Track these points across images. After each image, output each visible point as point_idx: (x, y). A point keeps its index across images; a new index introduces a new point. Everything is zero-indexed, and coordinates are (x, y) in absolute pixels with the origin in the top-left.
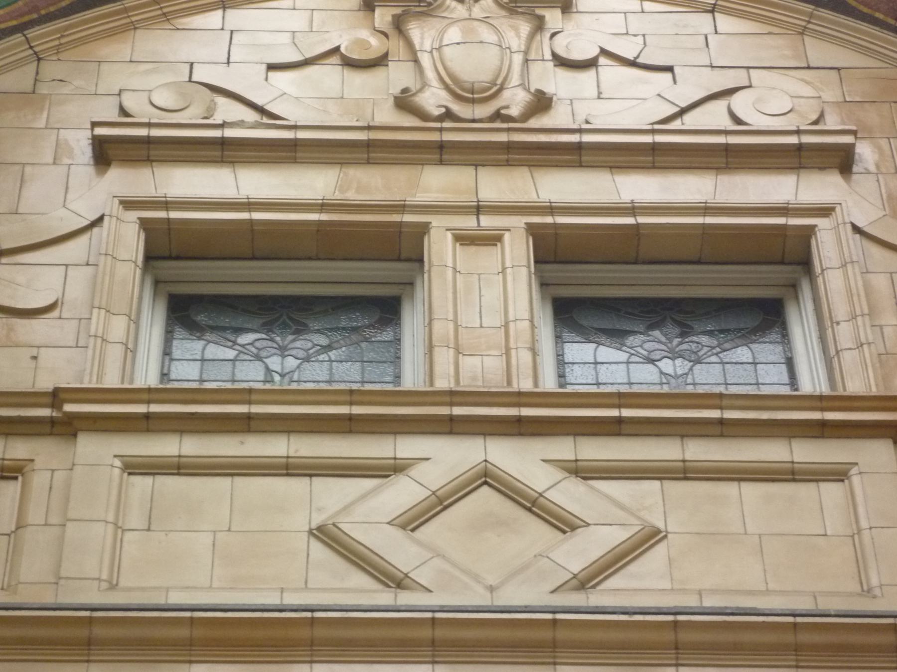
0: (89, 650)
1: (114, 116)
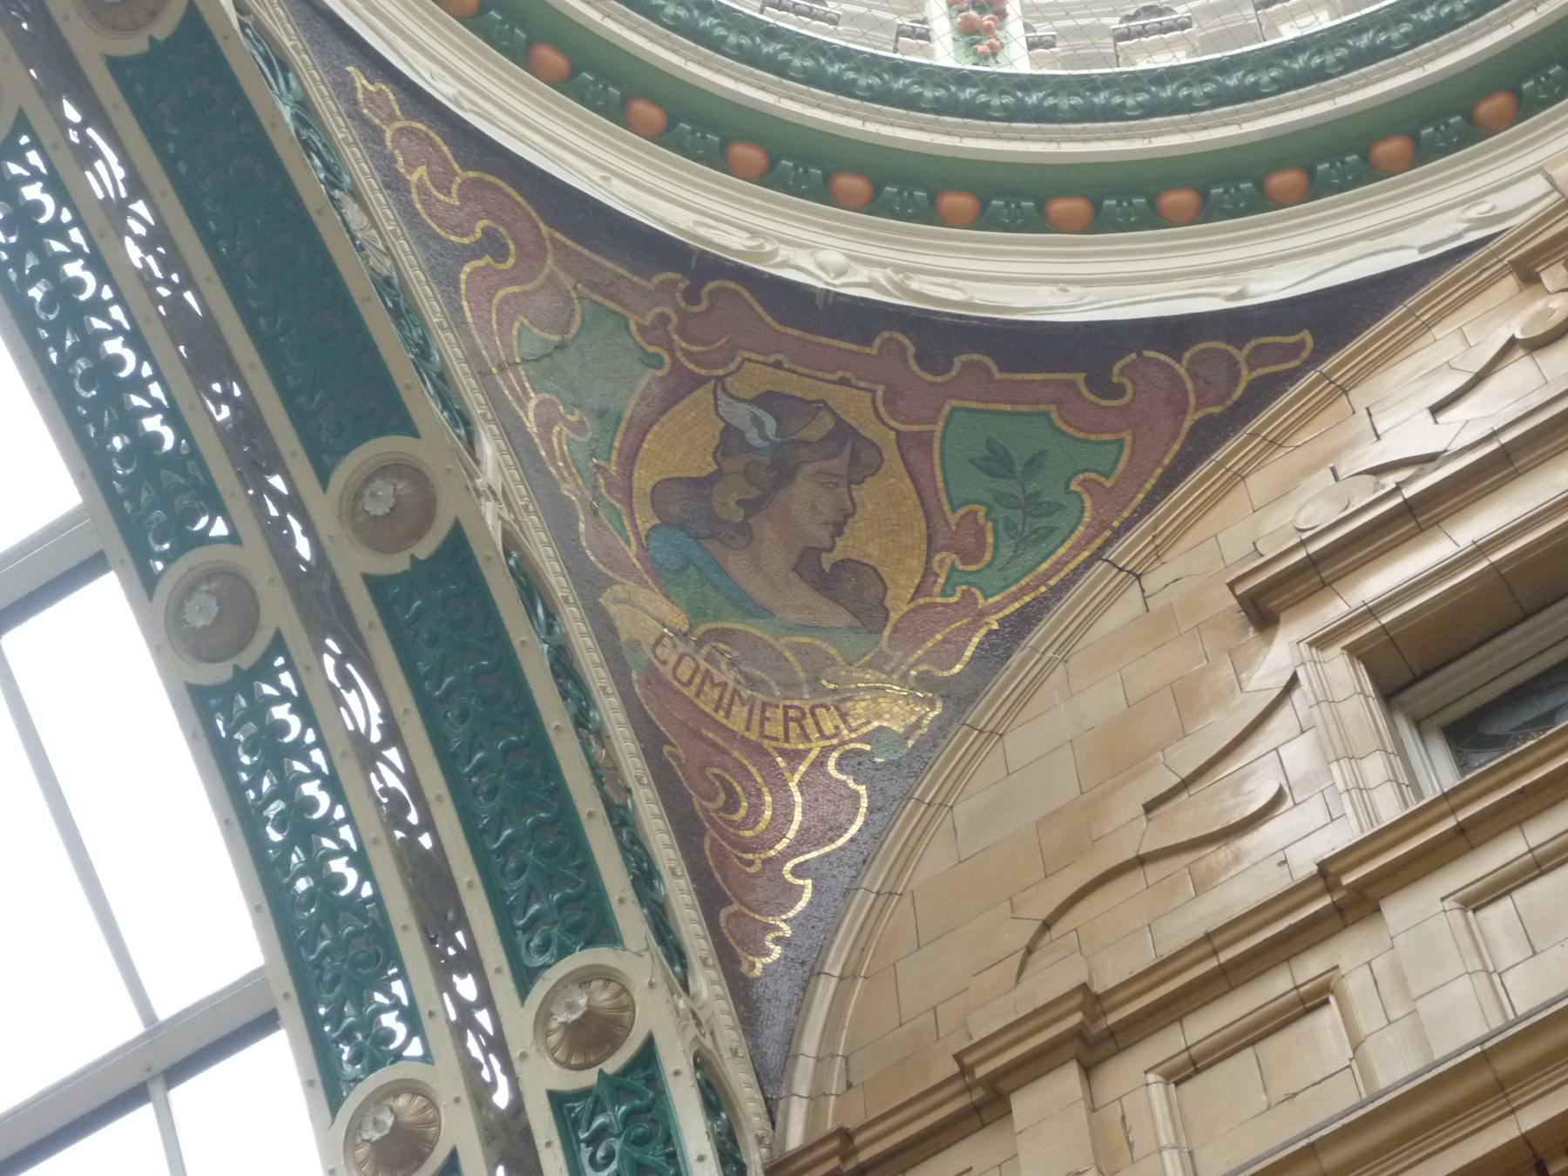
0: (1506, 1095)
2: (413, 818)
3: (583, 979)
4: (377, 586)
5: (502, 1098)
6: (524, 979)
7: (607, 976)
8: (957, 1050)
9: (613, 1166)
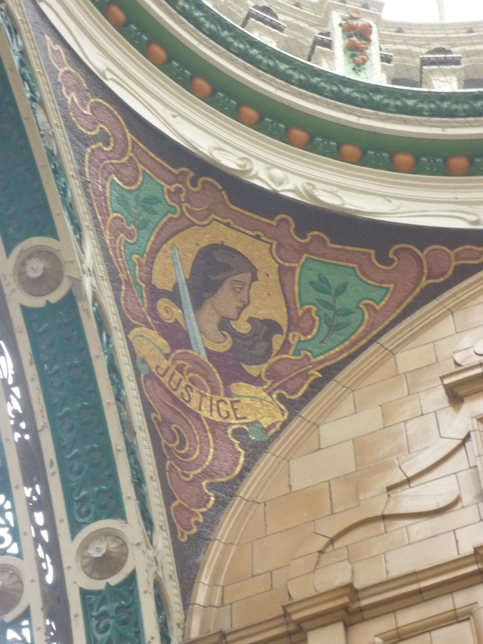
1: (454, 369)
4: (26, 311)
5: (50, 578)
6: (75, 528)
8: (284, 604)
9: (108, 633)
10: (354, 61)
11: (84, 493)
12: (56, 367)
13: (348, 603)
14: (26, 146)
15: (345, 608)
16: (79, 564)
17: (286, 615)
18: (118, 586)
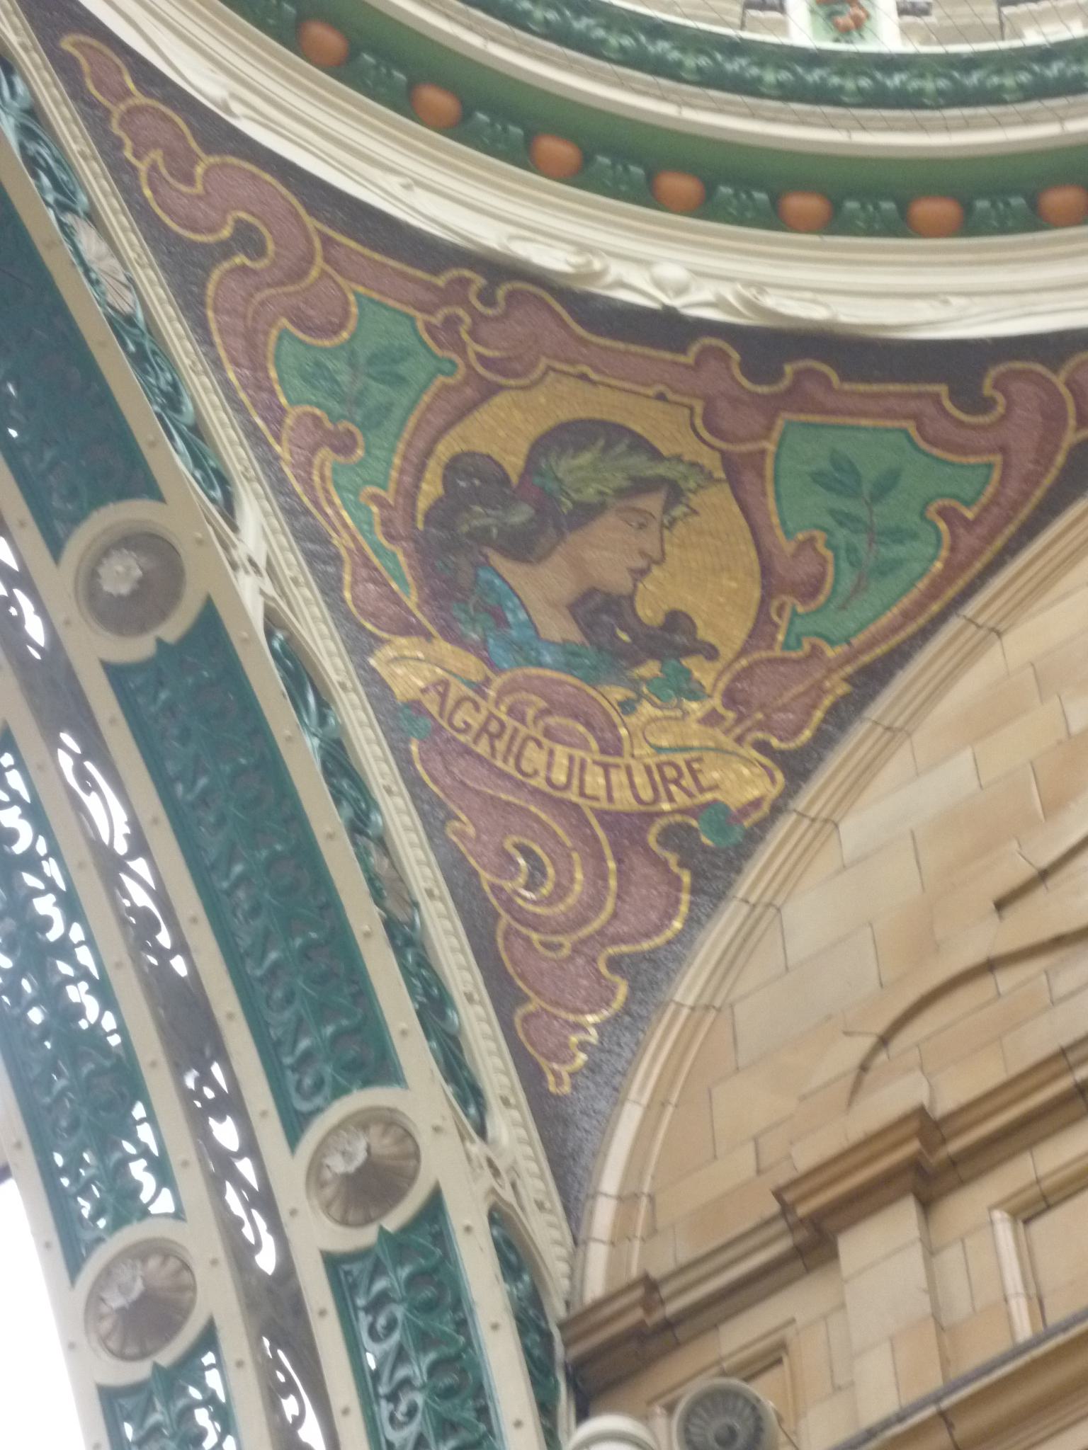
2: (164, 938)
3: (362, 1121)
4: (117, 674)
5: (267, 1260)
6: (294, 1126)
7: (389, 1120)
9: (396, 1337)
10: (837, 25)
11: (304, 1044)
12: (203, 782)
13: (920, 1153)
14: (59, 308)
15: (914, 1166)
16: (316, 1202)
17: (786, 1209)
18: (406, 1229)
